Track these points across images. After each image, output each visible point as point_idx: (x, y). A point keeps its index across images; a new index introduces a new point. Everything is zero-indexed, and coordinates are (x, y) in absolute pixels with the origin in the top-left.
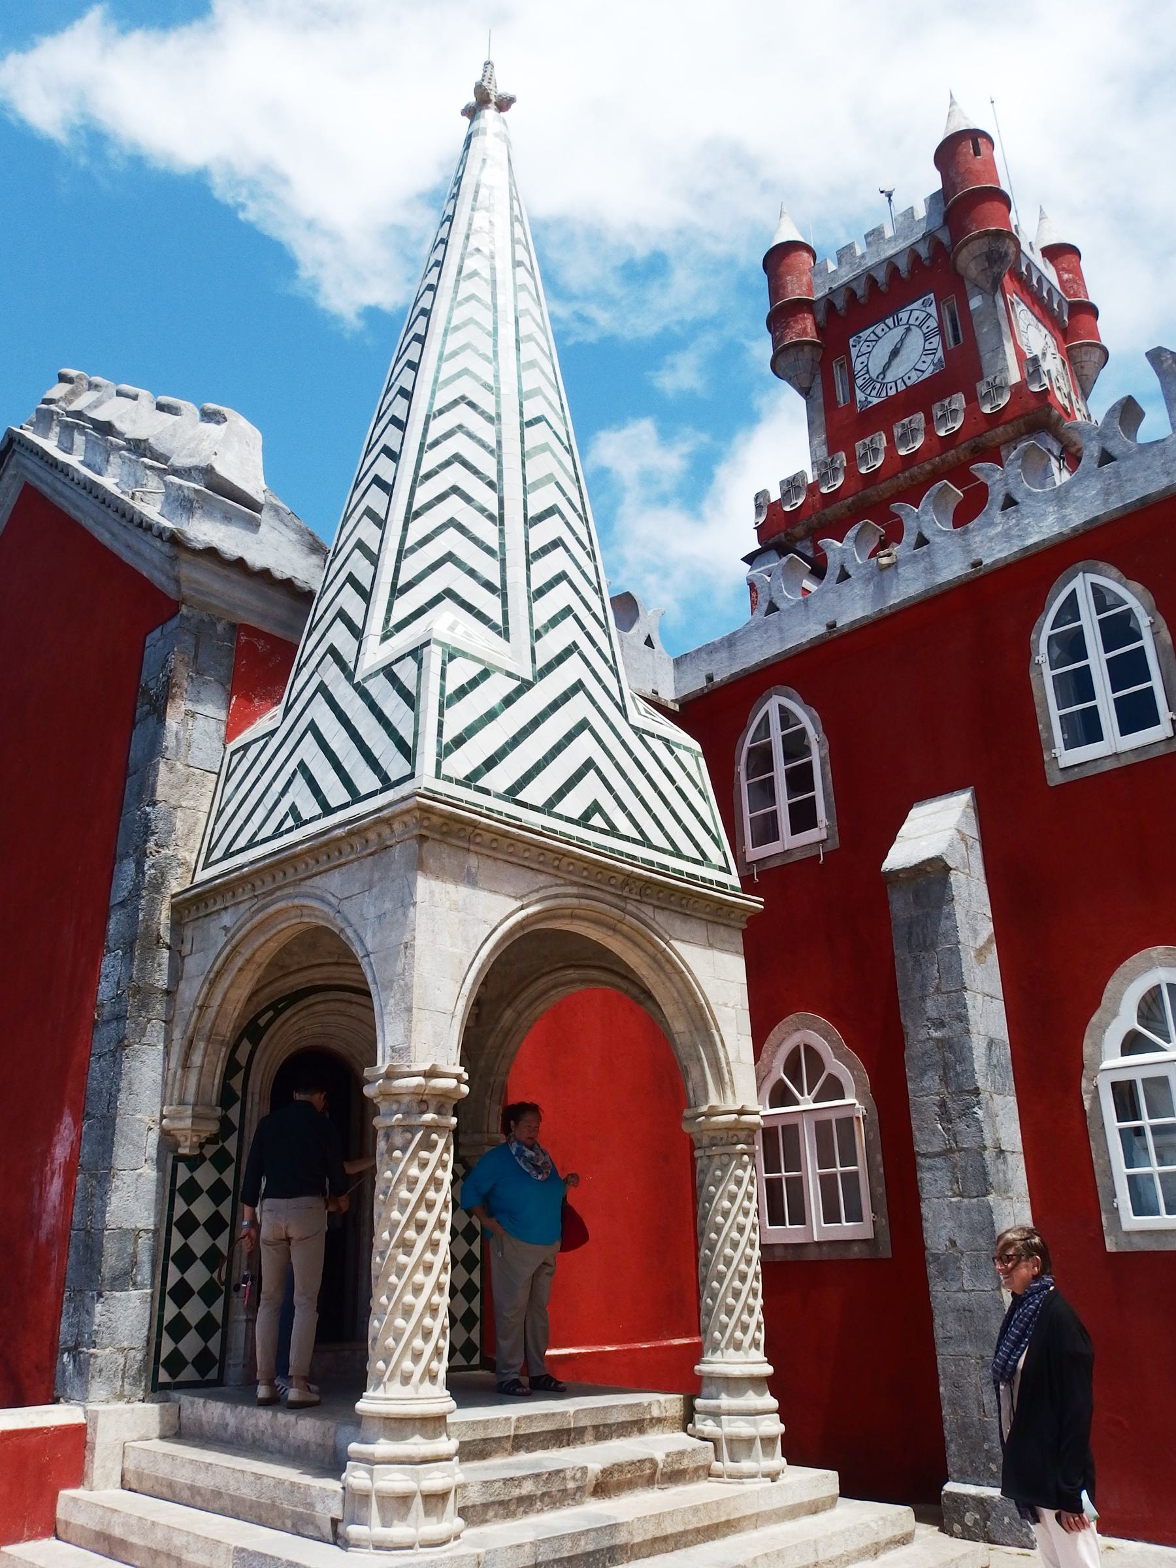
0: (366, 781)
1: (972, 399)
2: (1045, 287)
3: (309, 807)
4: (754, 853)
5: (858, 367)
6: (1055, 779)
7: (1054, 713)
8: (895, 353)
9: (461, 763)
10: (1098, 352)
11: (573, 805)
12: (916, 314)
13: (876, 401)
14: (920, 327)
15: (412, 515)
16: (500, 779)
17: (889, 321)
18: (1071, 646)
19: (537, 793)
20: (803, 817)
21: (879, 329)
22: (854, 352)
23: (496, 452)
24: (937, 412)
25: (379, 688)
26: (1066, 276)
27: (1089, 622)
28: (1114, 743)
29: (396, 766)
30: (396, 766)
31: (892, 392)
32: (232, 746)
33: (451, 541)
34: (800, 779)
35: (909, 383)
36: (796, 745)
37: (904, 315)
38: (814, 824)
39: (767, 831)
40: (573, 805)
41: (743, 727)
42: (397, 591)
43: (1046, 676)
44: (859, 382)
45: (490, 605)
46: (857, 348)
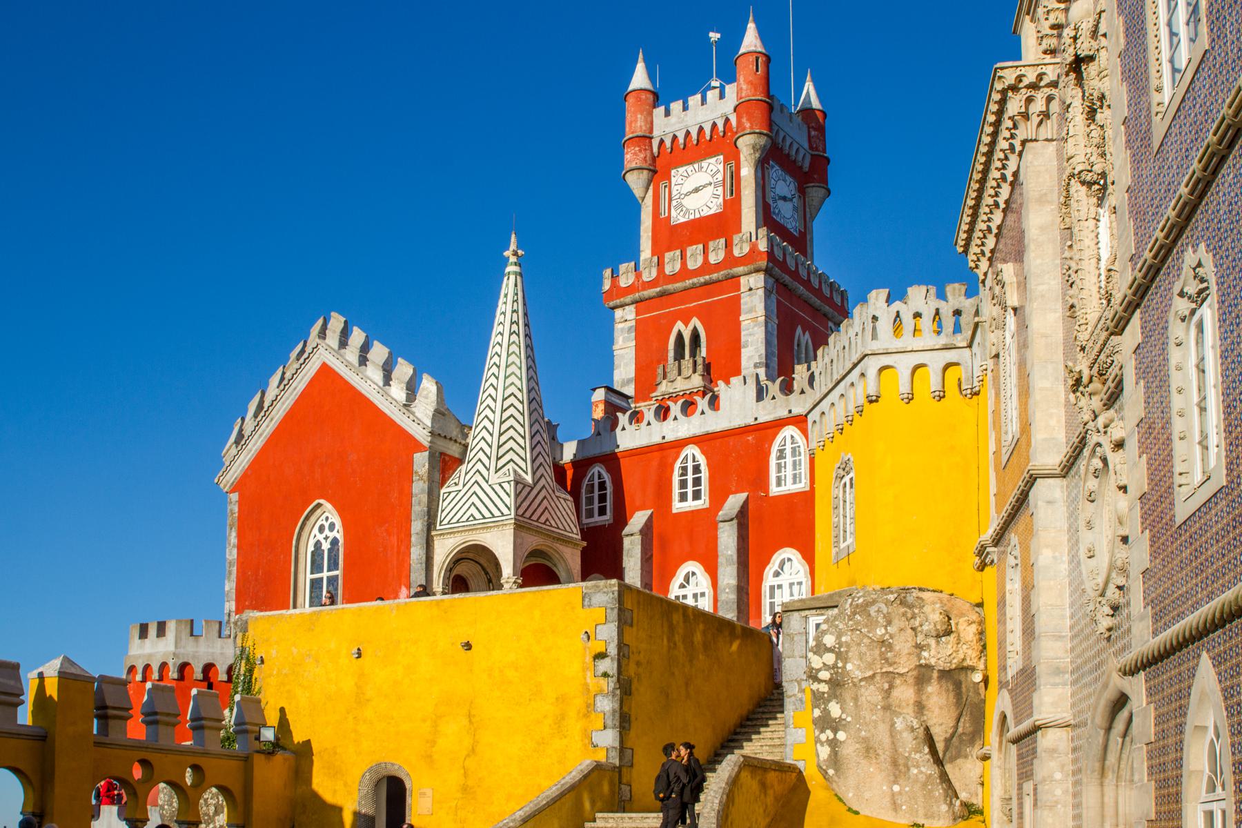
0: (497, 513)
1: (729, 246)
2: (795, 146)
3: (478, 516)
4: (585, 521)
5: (674, 193)
6: (674, 511)
7: (676, 490)
8: (697, 190)
9: (521, 511)
10: (823, 191)
11: (543, 519)
12: (711, 167)
13: (682, 220)
14: (713, 176)
15: (501, 435)
16: (528, 514)
17: (696, 166)
18: (685, 469)
19: (534, 518)
20: (602, 511)
21: (689, 168)
22: (673, 180)
23: (523, 414)
24: (711, 245)
25: (497, 488)
26: (813, 133)
27: (690, 465)
28: (691, 505)
29: (506, 511)
30: (506, 511)
31: (692, 217)
32: (442, 491)
33: (511, 444)
34: (602, 498)
35: (703, 214)
36: (602, 486)
37: (705, 164)
38: (605, 514)
39: (590, 514)
40: (543, 519)
41: (585, 476)
42: (498, 459)
43: (676, 479)
44: (674, 203)
45: (522, 464)
46: (677, 174)
